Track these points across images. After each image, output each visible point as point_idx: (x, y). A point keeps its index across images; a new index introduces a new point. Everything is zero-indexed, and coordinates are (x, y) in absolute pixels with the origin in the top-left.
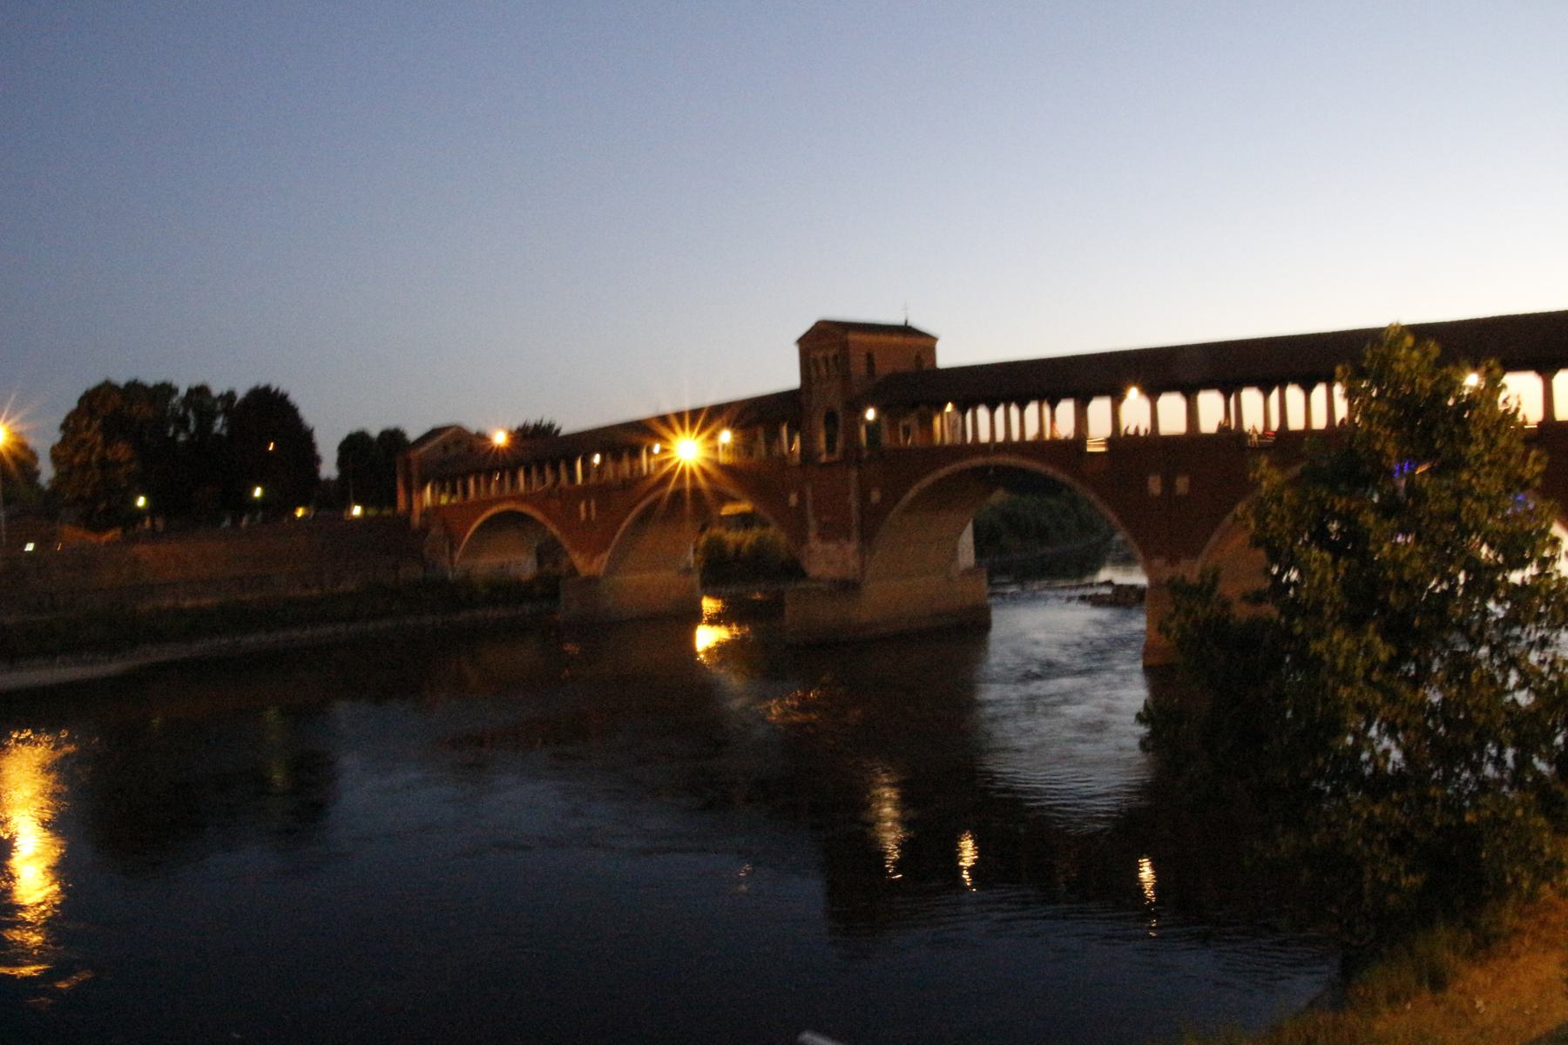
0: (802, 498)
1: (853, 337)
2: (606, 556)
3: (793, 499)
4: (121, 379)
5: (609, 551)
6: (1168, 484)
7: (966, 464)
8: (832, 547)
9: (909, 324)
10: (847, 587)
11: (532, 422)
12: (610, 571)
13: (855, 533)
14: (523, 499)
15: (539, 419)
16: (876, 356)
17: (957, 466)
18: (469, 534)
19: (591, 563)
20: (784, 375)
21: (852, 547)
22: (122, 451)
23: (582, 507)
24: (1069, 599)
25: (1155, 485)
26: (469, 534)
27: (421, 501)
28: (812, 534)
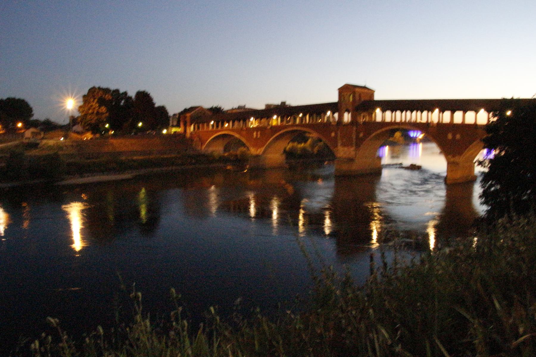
0: (336, 134)
1: (357, 90)
2: (263, 149)
3: (333, 134)
4: (97, 86)
5: (264, 147)
6: (454, 136)
7: (388, 128)
8: (346, 149)
9: (366, 86)
10: (351, 160)
11: (214, 107)
12: (264, 152)
13: (354, 145)
14: (232, 130)
15: (217, 105)
16: (362, 95)
17: (388, 128)
18: (209, 140)
19: (257, 151)
20: (334, 98)
21: (353, 149)
22: (103, 109)
23: (255, 134)
24: (396, 168)
25: (450, 136)
26: (209, 140)
27: (190, 129)
28: (339, 144)
